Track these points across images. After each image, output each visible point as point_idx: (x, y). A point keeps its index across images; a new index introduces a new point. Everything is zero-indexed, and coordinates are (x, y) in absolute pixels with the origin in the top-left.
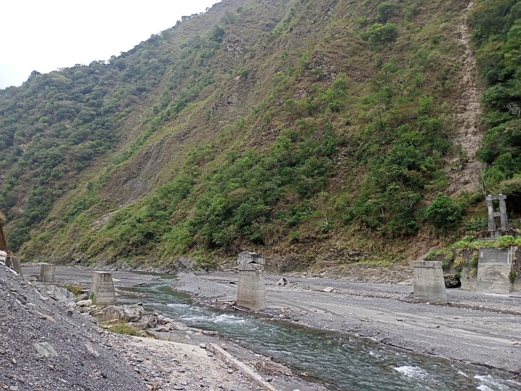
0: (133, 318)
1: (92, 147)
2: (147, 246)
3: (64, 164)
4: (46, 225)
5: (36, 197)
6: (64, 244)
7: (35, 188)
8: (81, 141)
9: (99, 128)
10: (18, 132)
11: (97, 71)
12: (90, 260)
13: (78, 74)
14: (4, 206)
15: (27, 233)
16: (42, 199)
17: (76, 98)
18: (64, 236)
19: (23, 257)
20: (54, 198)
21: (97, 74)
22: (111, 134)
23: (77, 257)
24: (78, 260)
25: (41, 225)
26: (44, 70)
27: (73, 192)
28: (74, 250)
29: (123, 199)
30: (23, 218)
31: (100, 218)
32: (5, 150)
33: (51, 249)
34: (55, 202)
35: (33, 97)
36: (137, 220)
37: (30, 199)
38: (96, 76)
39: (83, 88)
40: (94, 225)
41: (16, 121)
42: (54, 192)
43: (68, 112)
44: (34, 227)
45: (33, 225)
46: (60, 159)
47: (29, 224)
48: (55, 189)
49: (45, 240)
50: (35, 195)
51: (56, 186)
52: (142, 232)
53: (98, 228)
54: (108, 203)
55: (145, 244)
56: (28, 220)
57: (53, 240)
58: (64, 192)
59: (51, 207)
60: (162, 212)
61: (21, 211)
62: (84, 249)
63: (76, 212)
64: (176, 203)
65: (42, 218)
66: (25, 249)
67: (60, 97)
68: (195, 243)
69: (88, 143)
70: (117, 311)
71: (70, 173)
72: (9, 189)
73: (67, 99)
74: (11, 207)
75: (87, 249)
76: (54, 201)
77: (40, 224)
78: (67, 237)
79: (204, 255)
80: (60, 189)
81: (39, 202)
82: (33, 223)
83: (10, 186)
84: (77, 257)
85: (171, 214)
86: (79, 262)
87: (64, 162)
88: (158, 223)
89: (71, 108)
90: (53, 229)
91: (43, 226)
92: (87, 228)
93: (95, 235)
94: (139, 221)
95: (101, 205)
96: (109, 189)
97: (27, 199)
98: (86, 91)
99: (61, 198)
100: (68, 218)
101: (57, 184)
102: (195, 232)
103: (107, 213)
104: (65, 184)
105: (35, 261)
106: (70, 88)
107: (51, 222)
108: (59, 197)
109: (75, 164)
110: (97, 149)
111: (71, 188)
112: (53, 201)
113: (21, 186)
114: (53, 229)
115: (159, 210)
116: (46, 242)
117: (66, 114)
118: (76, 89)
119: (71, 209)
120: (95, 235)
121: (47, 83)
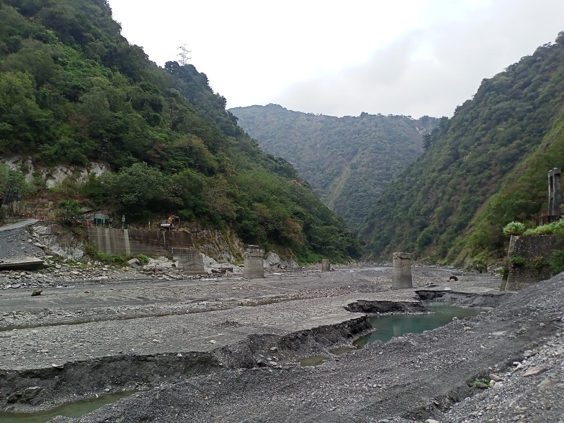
1: (519, 145)
3: (490, 169)
8: (510, 141)
9: (530, 123)
10: (461, 145)
11: (539, 58)
13: (519, 69)
16: (468, 207)
17: (515, 97)
21: (539, 61)
22: (543, 127)
26: (490, 76)
35: (476, 107)
38: (537, 64)
39: (522, 83)
41: (462, 135)
43: (503, 114)
46: (486, 166)
47: (456, 231)
48: (478, 196)
65: (466, 225)
67: (498, 100)
69: (515, 143)
71: (493, 178)
72: (449, 200)
73: (507, 100)
76: (478, 207)
80: (482, 195)
87: (490, 167)
89: (507, 108)
97: (460, 208)
98: (527, 85)
101: (481, 190)
104: (488, 190)
106: (511, 87)
109: (498, 169)
110: (523, 147)
113: (456, 196)
117: (502, 116)
118: (515, 87)
121: (488, 90)
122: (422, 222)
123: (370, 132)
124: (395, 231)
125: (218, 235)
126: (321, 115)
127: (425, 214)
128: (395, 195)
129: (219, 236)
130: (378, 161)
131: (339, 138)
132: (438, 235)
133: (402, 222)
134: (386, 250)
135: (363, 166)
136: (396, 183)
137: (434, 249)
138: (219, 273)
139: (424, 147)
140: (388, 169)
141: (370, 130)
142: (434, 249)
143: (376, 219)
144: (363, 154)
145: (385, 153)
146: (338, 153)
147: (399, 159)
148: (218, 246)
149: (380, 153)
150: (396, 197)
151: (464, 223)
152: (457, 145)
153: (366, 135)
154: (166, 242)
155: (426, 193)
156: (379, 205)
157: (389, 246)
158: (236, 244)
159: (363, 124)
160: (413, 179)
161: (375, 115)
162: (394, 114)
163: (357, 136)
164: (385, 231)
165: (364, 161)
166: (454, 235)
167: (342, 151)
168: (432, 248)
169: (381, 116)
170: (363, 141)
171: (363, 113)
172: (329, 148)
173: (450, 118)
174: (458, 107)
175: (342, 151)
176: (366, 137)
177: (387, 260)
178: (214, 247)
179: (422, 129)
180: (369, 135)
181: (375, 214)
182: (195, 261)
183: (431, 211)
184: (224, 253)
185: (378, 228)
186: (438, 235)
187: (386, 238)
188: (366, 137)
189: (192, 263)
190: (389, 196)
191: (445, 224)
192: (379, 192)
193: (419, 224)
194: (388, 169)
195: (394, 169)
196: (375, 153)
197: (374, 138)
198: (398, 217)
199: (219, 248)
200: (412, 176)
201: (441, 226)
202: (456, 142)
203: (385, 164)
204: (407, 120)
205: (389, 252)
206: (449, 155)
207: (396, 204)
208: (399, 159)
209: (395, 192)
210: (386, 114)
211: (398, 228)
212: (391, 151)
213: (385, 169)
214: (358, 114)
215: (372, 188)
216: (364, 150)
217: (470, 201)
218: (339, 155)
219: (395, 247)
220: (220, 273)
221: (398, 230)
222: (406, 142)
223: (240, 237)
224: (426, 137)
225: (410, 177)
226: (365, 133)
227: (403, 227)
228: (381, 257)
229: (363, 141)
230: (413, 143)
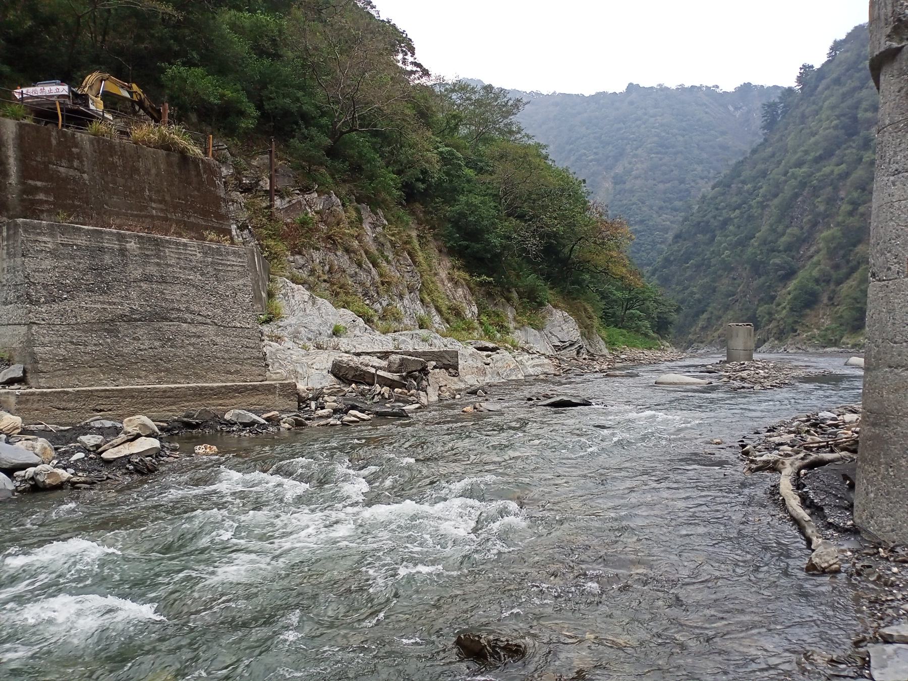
10: (864, 105)
32: (844, 146)
72: (851, 214)
74: (855, 246)
122: (786, 262)
123: (646, 117)
124: (716, 287)
125: (374, 226)
126: (555, 93)
127: (789, 248)
128: (712, 220)
129: (379, 229)
130: (663, 168)
131: (589, 131)
132: (832, 287)
133: (732, 269)
134: (701, 324)
135: (636, 178)
136: (711, 198)
137: (824, 314)
138: (384, 382)
139: (764, 128)
140: (682, 181)
141: (645, 114)
142: (824, 314)
143: (673, 268)
144: (635, 156)
145: (676, 153)
146: (590, 158)
147: (701, 162)
148: (375, 264)
149: (666, 153)
150: (714, 223)
152: (856, 107)
153: (638, 123)
154: (28, 190)
155: (786, 209)
156: (677, 242)
157: (705, 316)
158: (443, 274)
159: (631, 103)
160: (746, 187)
161: (652, 88)
162: (688, 85)
163: (621, 125)
164: (695, 290)
165: (637, 169)
167: (596, 154)
168: (821, 312)
169: (663, 89)
170: (633, 133)
171: (631, 84)
172: (571, 150)
173: (817, 66)
174: (835, 41)
175: (596, 154)
176: (639, 126)
177: (702, 342)
178: (360, 265)
179: (741, 108)
180: (644, 123)
181: (672, 258)
182: (175, 292)
183: (805, 240)
184: (401, 297)
185: (677, 284)
186: (832, 287)
187: (699, 301)
188: (639, 126)
189: (135, 301)
190: (699, 223)
191: (848, 262)
192: (668, 223)
193: (780, 267)
194: (682, 181)
195: (694, 181)
196: (657, 153)
197: (654, 127)
198: (723, 261)
199: (381, 275)
200: (744, 182)
201: (837, 267)
202: (850, 102)
203: (676, 172)
204: (711, 93)
205: (706, 327)
206: (836, 127)
207: (714, 237)
208: (701, 162)
209: (710, 215)
210: (672, 84)
211: (725, 281)
212: (686, 148)
213: (676, 182)
214: (621, 88)
215: (654, 216)
216: (637, 149)
218: (591, 161)
219: (720, 317)
220: (392, 384)
221: (724, 285)
222: (712, 132)
223: (451, 252)
224: (769, 106)
225: (740, 185)
226: (637, 120)
227: (735, 279)
228: (690, 336)
229: (633, 133)
230: (723, 133)
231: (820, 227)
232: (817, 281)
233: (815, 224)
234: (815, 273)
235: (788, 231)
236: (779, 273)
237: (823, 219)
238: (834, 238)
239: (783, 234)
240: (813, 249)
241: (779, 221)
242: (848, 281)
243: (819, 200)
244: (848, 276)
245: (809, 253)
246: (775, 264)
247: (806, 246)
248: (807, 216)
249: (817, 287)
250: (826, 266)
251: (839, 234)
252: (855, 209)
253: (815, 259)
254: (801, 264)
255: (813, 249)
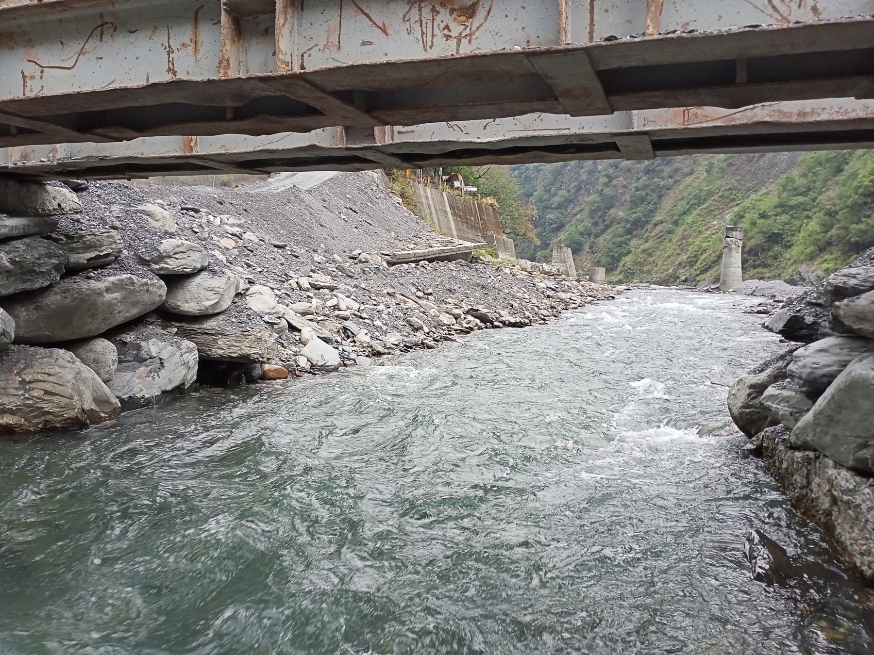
0: (549, 272)
2: (770, 254)
4: (651, 232)
5: (638, 193)
6: (669, 257)
7: (639, 179)
12: (698, 278)
14: (600, 210)
15: (627, 244)
16: (647, 195)
18: (670, 247)
19: (621, 277)
20: (661, 193)
23: (683, 273)
24: (683, 278)
25: (645, 233)
27: (688, 180)
28: (680, 264)
29: (758, 184)
30: (623, 224)
31: (719, 216)
33: (654, 265)
34: (663, 197)
36: (760, 214)
37: (631, 197)
40: (710, 228)
42: (662, 183)
44: (635, 236)
45: (634, 233)
47: (629, 232)
48: (663, 178)
49: (648, 253)
50: (637, 189)
51: (665, 174)
52: (763, 233)
53: (714, 231)
54: (734, 192)
55: (768, 250)
56: (628, 226)
57: (658, 253)
58: (675, 182)
59: (658, 206)
60: (801, 199)
61: (621, 214)
62: (691, 263)
63: (688, 210)
64: (825, 181)
65: (647, 222)
66: (624, 266)
68: (829, 244)
70: (538, 267)
72: (606, 185)
74: (609, 209)
75: (696, 262)
76: (663, 195)
77: (643, 231)
78: (674, 247)
79: (839, 262)
80: (670, 177)
81: (642, 200)
82: (635, 229)
83: (606, 180)
84: (683, 273)
85: (814, 200)
86: (686, 280)
88: (793, 217)
90: (659, 238)
91: (648, 234)
92: (700, 232)
93: (709, 241)
94: (763, 216)
95: (722, 196)
96: (737, 169)
97: (628, 197)
99: (672, 191)
100: (679, 219)
102: (832, 226)
103: (731, 207)
105: (635, 281)
107: (659, 228)
108: (669, 189)
111: (686, 175)
112: (660, 197)
113: (621, 179)
114: (659, 238)
115: (798, 195)
116: (650, 255)
119: (682, 206)
120: (709, 241)
127: (559, 207)
151: (643, 219)
166: (625, 237)
186: (593, 239)
201: (596, 224)
217: (649, 185)
231: (582, 192)
232: (581, 234)
233: (579, 189)
234: (580, 228)
235: (560, 193)
236: (552, 226)
237: (585, 186)
238: (594, 202)
239: (555, 195)
240: (577, 209)
241: (552, 184)
242: (604, 235)
243: (583, 170)
244: (603, 231)
245: (574, 212)
246: (550, 219)
247: (572, 205)
248: (573, 182)
249: (582, 239)
250: (588, 223)
251: (598, 199)
252: (610, 181)
253: (578, 216)
254: (568, 219)
255: (577, 209)
